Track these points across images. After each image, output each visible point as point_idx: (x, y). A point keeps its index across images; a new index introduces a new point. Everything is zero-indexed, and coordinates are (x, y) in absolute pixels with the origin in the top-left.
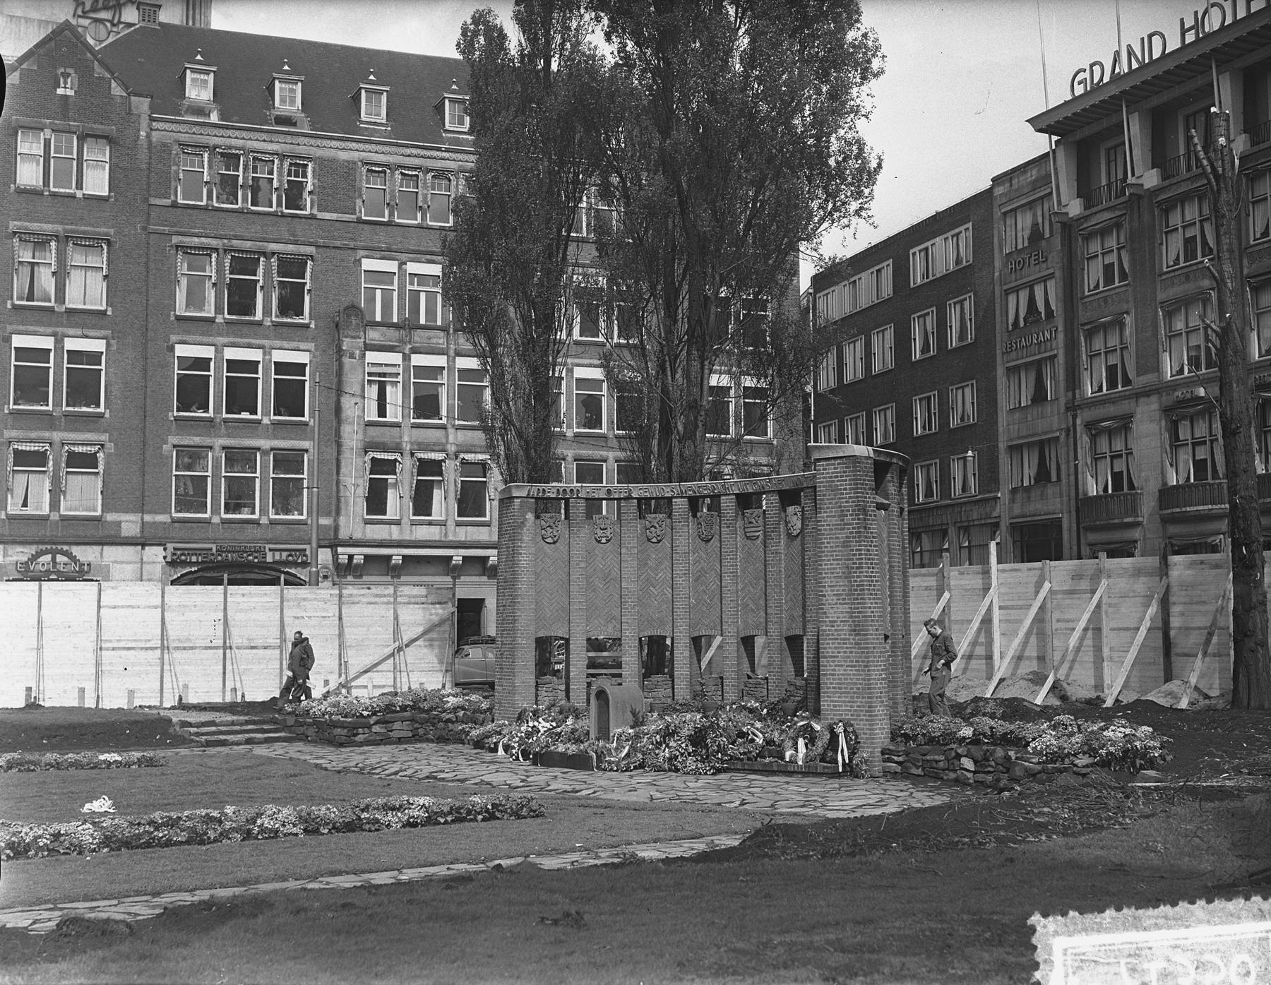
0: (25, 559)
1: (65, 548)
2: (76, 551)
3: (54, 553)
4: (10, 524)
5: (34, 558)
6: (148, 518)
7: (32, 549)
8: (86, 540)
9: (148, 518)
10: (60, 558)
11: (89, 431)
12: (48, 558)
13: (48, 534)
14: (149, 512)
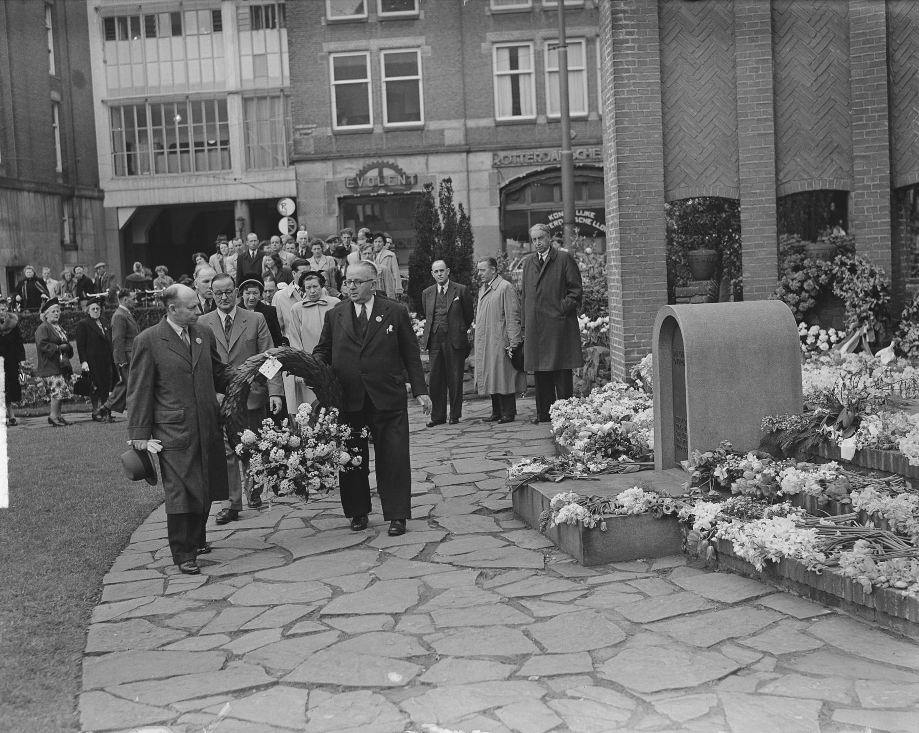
0: (353, 175)
1: (391, 161)
2: (402, 163)
3: (381, 167)
4: (336, 139)
5: (362, 173)
6: (471, 123)
7: (359, 165)
8: (410, 151)
9: (471, 123)
10: (387, 172)
11: (405, 36)
12: (374, 173)
13: (374, 147)
14: (472, 117)
